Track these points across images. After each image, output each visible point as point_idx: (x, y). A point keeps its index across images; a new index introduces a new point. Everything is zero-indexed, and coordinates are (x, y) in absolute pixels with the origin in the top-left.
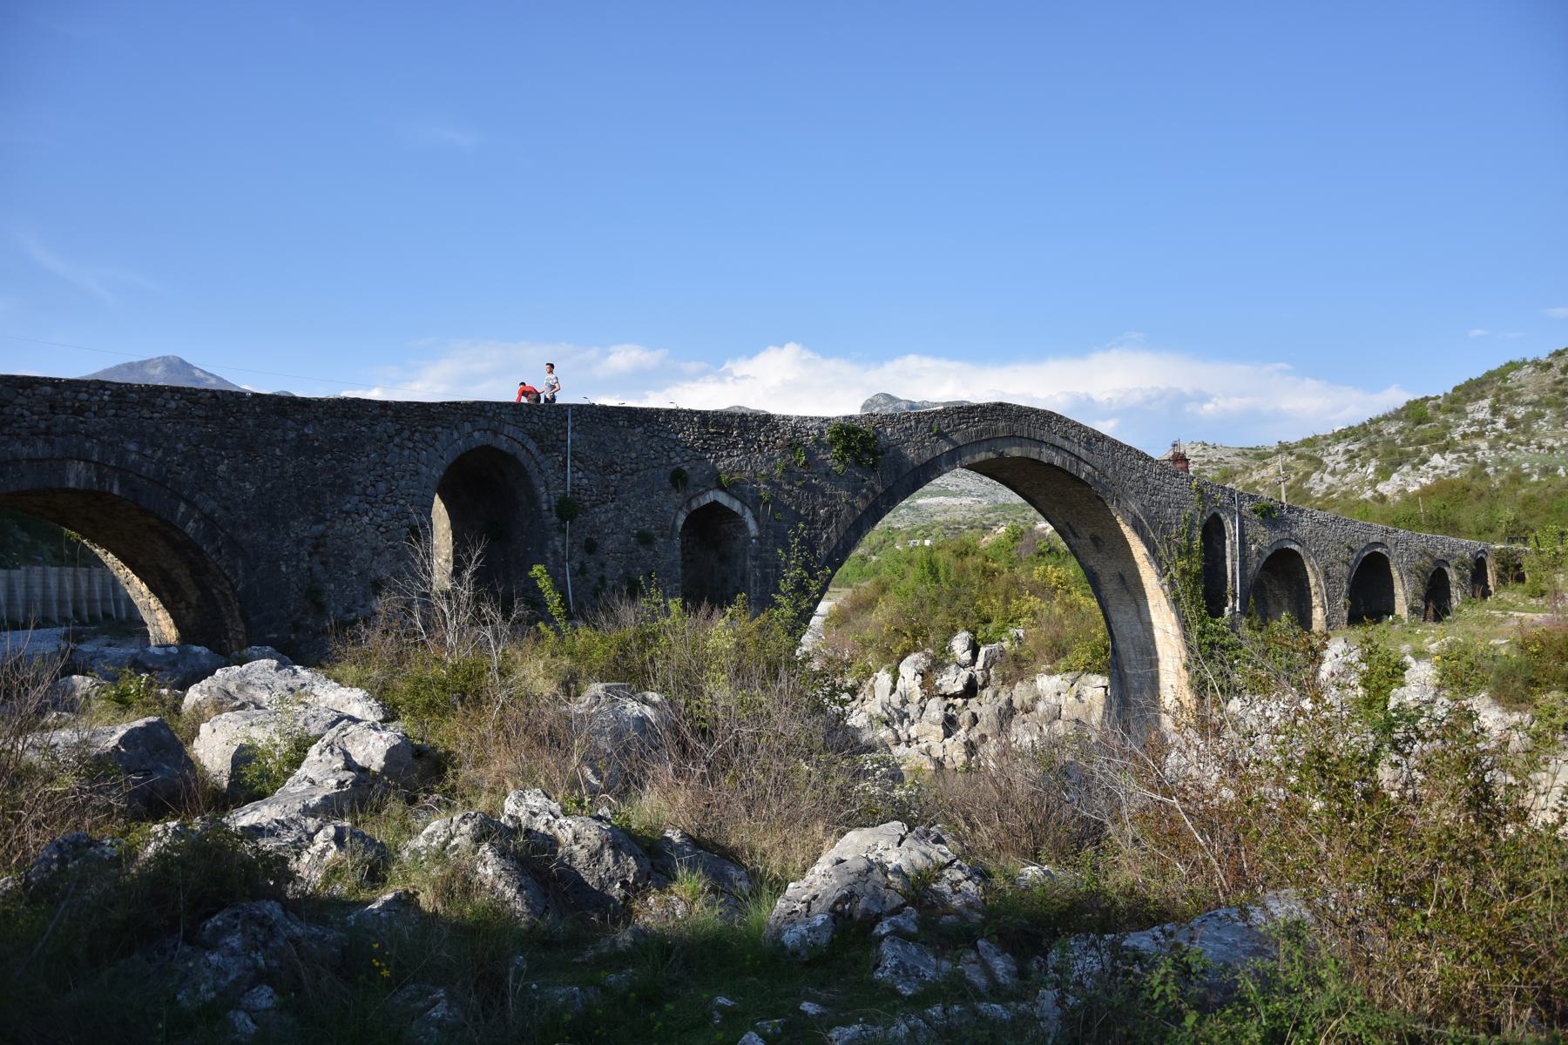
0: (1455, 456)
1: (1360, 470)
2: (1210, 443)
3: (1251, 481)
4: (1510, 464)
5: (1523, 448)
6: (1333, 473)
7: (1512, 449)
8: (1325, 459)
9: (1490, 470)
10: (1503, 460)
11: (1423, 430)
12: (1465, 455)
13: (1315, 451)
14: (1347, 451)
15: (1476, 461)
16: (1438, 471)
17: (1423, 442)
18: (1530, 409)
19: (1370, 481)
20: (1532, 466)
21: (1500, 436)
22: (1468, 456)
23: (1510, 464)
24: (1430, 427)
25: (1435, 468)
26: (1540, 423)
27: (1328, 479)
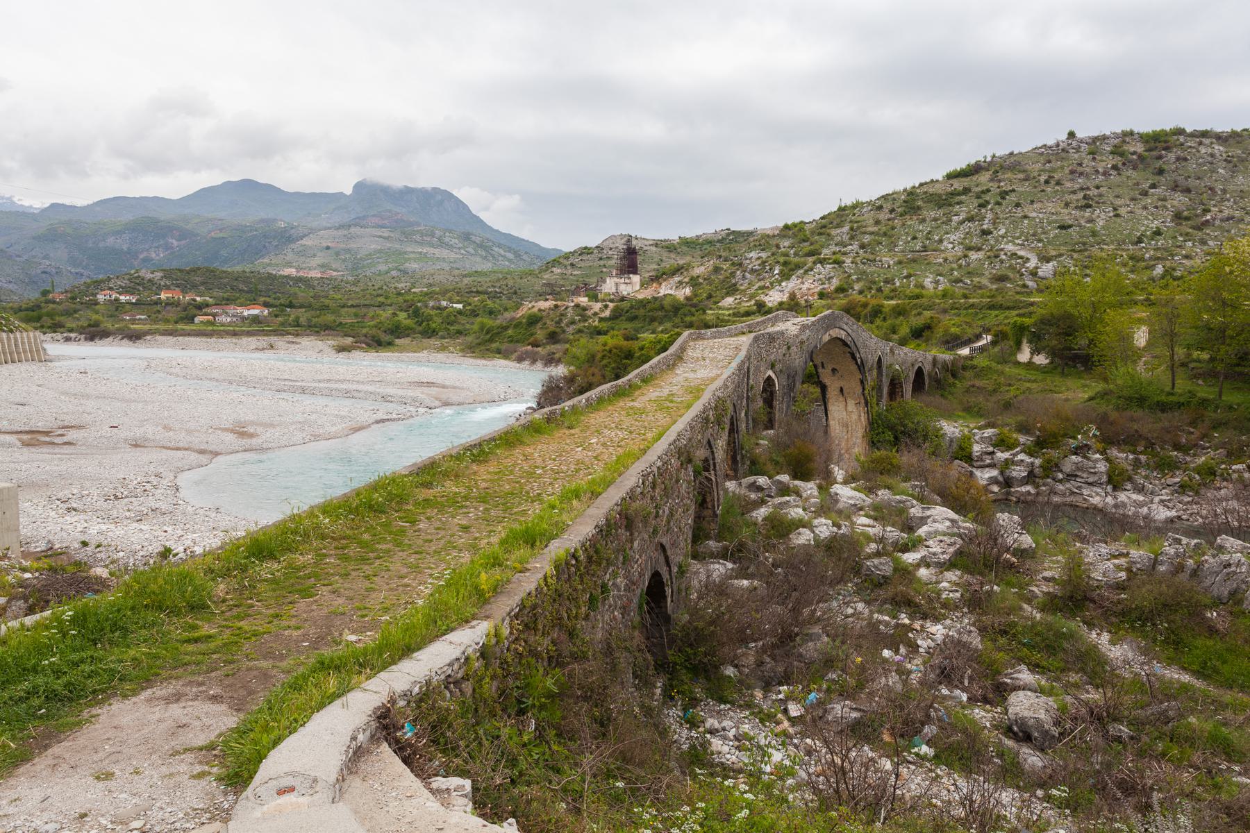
18: (873, 237)
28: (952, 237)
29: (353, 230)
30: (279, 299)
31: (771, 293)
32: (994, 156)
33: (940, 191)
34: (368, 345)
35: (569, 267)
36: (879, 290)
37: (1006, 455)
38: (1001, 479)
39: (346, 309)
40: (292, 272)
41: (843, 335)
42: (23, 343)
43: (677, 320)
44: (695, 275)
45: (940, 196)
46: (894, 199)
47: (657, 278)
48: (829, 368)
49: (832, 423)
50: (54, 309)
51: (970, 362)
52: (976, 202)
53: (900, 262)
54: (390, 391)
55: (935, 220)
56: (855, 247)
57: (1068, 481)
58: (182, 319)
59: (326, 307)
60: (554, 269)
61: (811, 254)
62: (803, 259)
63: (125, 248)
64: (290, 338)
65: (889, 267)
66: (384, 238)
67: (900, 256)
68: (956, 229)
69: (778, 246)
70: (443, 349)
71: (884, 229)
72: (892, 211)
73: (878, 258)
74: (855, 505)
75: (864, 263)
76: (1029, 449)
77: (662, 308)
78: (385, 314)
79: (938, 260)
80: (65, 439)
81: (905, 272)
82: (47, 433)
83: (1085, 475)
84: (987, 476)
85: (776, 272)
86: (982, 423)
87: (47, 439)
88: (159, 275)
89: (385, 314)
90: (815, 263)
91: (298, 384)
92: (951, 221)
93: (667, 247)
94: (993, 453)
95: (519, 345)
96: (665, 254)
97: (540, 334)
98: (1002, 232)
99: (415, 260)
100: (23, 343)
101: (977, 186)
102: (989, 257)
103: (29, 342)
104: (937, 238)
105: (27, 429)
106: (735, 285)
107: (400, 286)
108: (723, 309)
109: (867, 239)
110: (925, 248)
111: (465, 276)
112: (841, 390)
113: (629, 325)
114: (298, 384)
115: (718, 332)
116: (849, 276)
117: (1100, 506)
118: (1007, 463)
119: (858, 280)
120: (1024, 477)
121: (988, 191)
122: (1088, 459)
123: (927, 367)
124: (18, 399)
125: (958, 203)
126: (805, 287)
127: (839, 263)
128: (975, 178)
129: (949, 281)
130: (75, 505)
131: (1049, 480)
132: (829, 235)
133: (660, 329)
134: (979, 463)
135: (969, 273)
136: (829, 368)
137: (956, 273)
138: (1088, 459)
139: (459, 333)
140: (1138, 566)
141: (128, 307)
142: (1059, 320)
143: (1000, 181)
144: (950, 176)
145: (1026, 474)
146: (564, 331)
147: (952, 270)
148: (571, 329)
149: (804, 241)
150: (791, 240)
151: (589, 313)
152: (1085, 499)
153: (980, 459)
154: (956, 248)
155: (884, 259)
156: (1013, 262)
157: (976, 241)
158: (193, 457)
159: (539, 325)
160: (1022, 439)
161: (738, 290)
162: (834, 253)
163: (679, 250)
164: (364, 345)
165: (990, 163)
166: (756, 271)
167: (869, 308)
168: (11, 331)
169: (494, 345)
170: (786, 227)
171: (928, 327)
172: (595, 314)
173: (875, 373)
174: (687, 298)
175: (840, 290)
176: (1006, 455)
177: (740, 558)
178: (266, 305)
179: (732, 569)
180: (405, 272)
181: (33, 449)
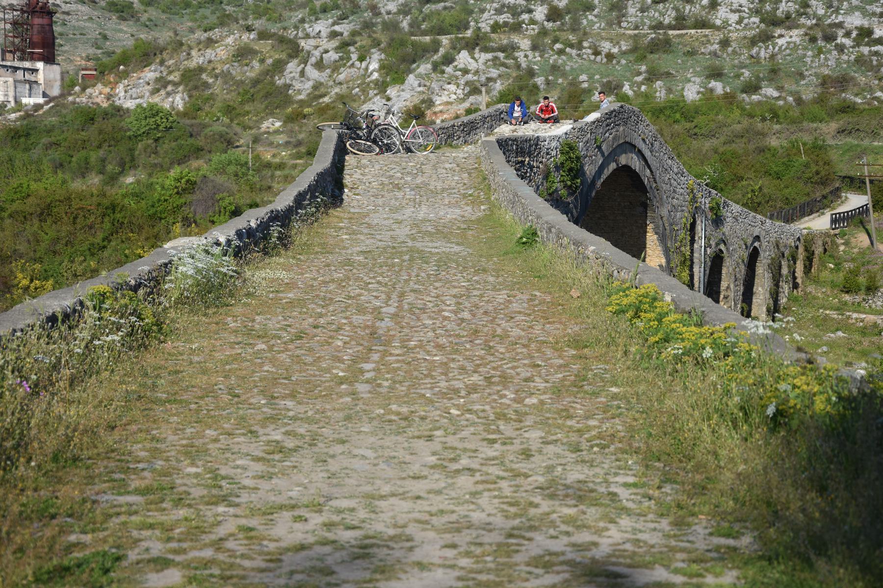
0: (489, 56)
1: (358, 64)
3: (193, 64)
4: (564, 75)
5: (574, 52)
6: (320, 65)
7: (561, 52)
8: (302, 43)
9: (540, 81)
10: (555, 69)
11: (438, 13)
12: (501, 55)
13: (285, 29)
14: (334, 35)
15: (518, 66)
16: (470, 77)
17: (442, 31)
19: (376, 82)
20: (591, 77)
21: (544, 32)
22: (506, 57)
23: (564, 75)
24: (445, 8)
25: (466, 71)
26: (590, 17)
27: (313, 73)
156: (865, 50)
163: (144, 17)
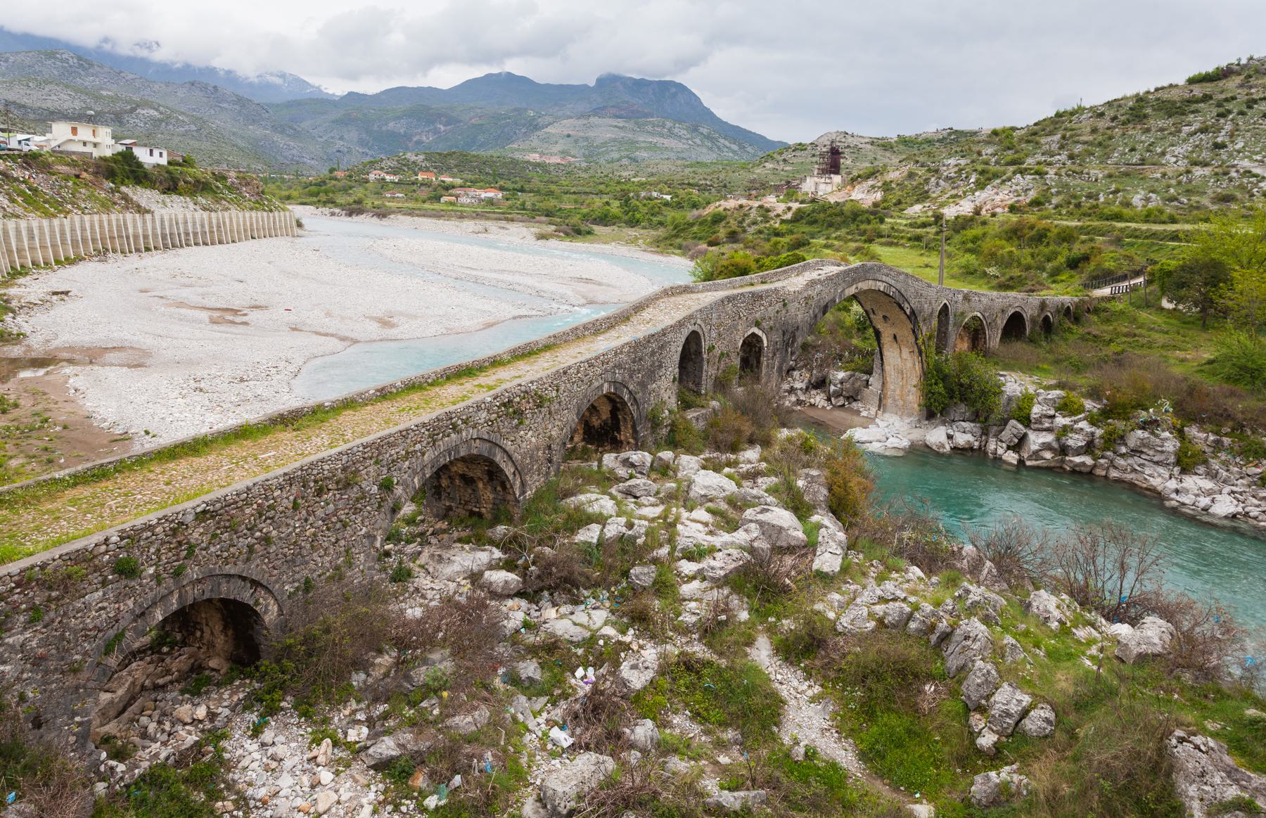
2: (850, 133)
18: (1086, 146)
28: (1178, 150)
29: (592, 119)
30: (515, 182)
31: (962, 202)
32: (1251, 58)
33: (1176, 98)
34: (567, 234)
35: (781, 163)
36: (1078, 206)
37: (1066, 421)
38: (1055, 445)
39: (568, 196)
40: (534, 157)
41: (881, 286)
42: (280, 221)
43: (853, 227)
44: (888, 180)
45: (1175, 102)
46: (1120, 106)
47: (854, 181)
48: (880, 314)
49: (887, 368)
50: (334, 186)
51: (1103, 304)
52: (1215, 111)
53: (1110, 176)
54: (548, 286)
55: (1162, 130)
56: (1063, 157)
57: (1132, 456)
58: (430, 199)
59: (551, 193)
60: (767, 164)
61: (1013, 163)
62: (1003, 168)
63: (402, 131)
64: (503, 223)
65: (1096, 180)
66: (619, 127)
67: (1111, 169)
68: (1184, 141)
69: (979, 154)
70: (633, 241)
71: (1100, 138)
72: (1114, 119)
73: (1086, 171)
74: (705, 496)
75: (1068, 176)
76: (1092, 418)
77: (842, 213)
78: (598, 202)
79: (1155, 175)
80: (244, 319)
81: (1113, 187)
82: (235, 312)
83: (1151, 453)
84: (1041, 440)
85: (972, 180)
86: (1053, 382)
87: (231, 318)
88: (422, 157)
89: (598, 202)
90: (1014, 173)
91: (474, 273)
92: (1180, 131)
93: (883, 146)
94: (1053, 417)
95: (701, 242)
96: (880, 152)
97: (722, 233)
98: (1240, 145)
99: (645, 149)
100: (280, 221)
101: (1222, 92)
102: (1216, 174)
103: (285, 220)
104: (1159, 150)
105: (225, 306)
106: (927, 192)
107: (624, 174)
108: (903, 218)
109: (1078, 149)
110: (1143, 161)
111: (687, 166)
112: (895, 337)
113: (807, 229)
114: (474, 273)
115: (714, 284)
116: (1049, 189)
117: (1159, 488)
118: (1065, 430)
119: (1058, 193)
120: (1081, 447)
121: (1233, 98)
122: (1157, 436)
123: (1030, 312)
124: (240, 279)
125: (1193, 112)
126: (998, 198)
127: (1041, 174)
128: (1221, 83)
129: (1162, 199)
130: (202, 385)
131: (1109, 453)
132: (1037, 143)
133: (834, 235)
134: (1036, 426)
135: (1188, 191)
136: (880, 314)
137: (1172, 190)
138: (1157, 436)
139: (661, 223)
140: (890, 618)
141: (391, 185)
142: (1202, 269)
143: (1251, 87)
144: (1192, 81)
145: (1083, 443)
146: (745, 231)
147: (1169, 187)
148: (752, 229)
149: (1009, 148)
150: (996, 147)
151: (772, 214)
152: (1146, 479)
153: (1039, 421)
154: (1179, 163)
155: (1092, 172)
156: (1245, 180)
157: (1205, 155)
158: (333, 344)
159: (723, 223)
160: (1089, 404)
161: (929, 197)
162: (1039, 163)
163: (895, 149)
164: (562, 234)
165: (1244, 67)
166: (951, 178)
167: (1034, 232)
168: (271, 211)
169: (679, 240)
170: (995, 133)
171: (1086, 258)
172: (778, 216)
173: (935, 322)
174: (875, 205)
175: (1036, 203)
176: (1066, 421)
177: (510, 549)
178: (502, 189)
179: (500, 559)
180: (635, 160)
181: (216, 327)
